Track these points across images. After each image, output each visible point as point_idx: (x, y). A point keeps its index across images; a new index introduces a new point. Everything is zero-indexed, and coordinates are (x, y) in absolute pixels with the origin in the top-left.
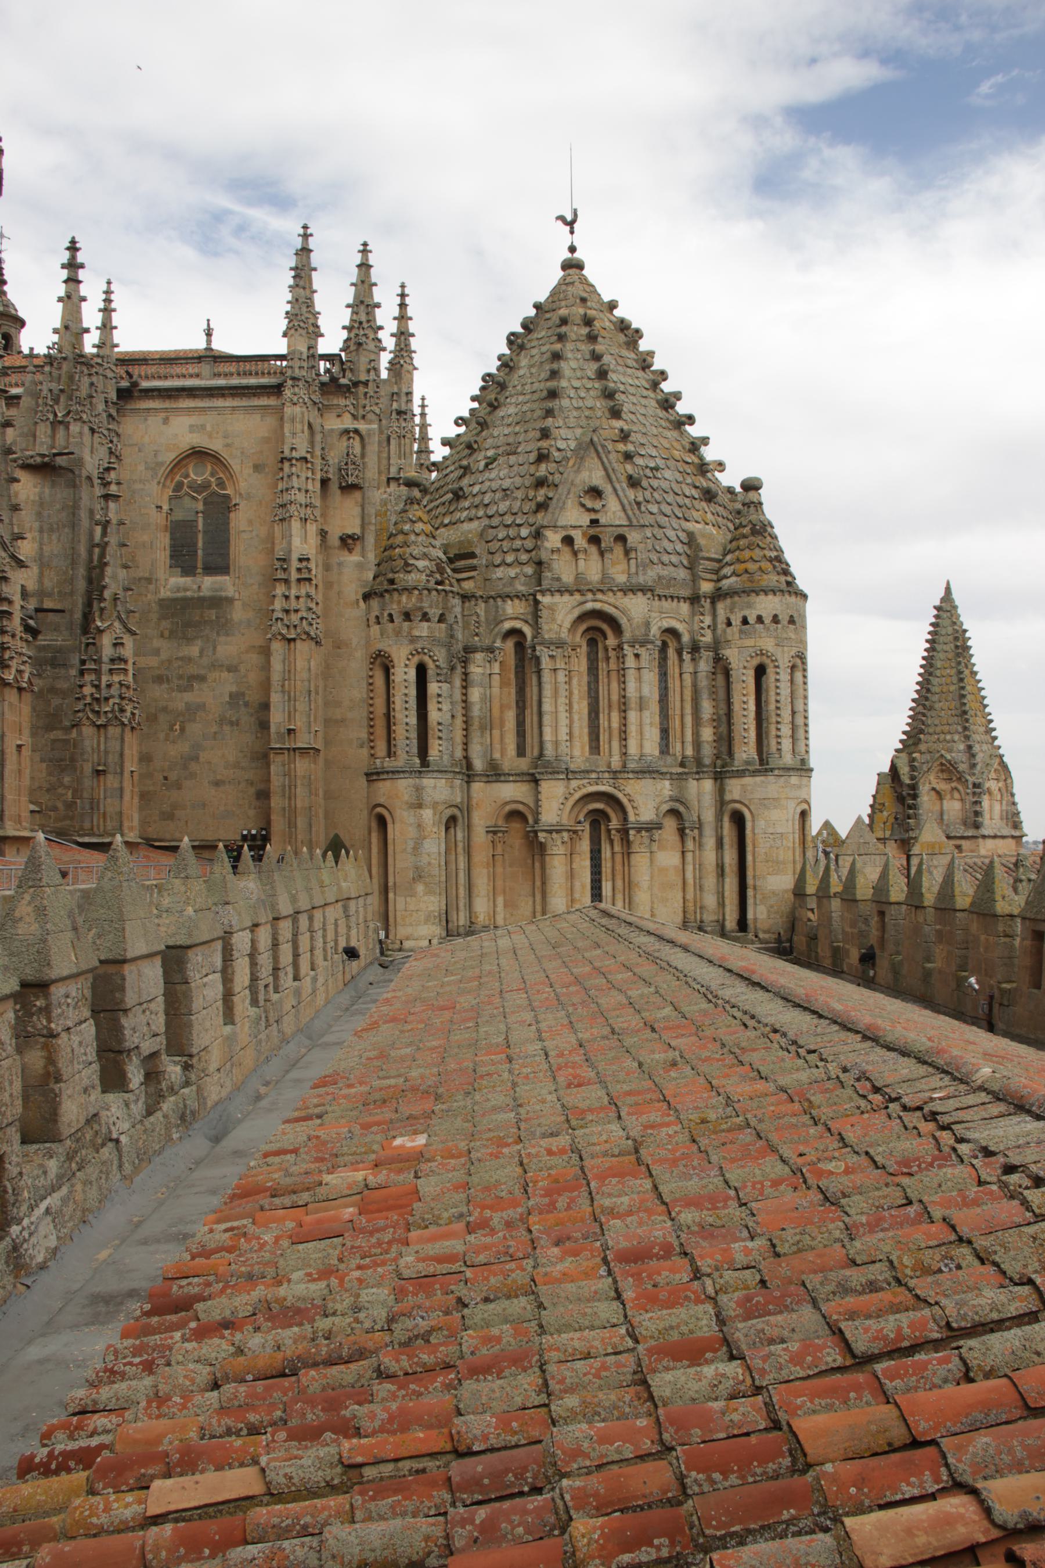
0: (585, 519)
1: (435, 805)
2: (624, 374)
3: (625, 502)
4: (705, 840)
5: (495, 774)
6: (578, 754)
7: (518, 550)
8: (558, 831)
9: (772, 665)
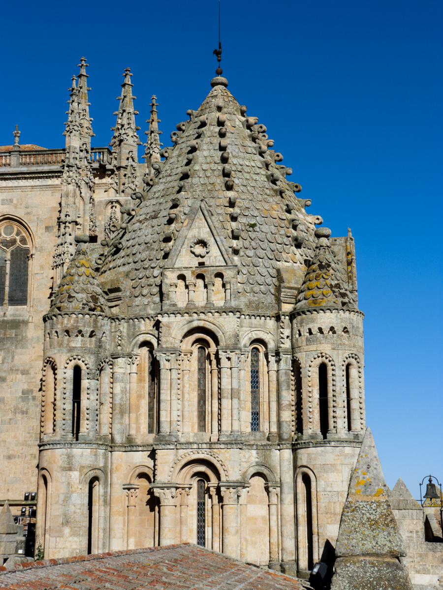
0: (195, 262)
1: (82, 467)
2: (244, 158)
3: (223, 249)
4: (284, 496)
5: (130, 445)
6: (188, 429)
7: (151, 285)
8: (168, 488)
9: (330, 364)
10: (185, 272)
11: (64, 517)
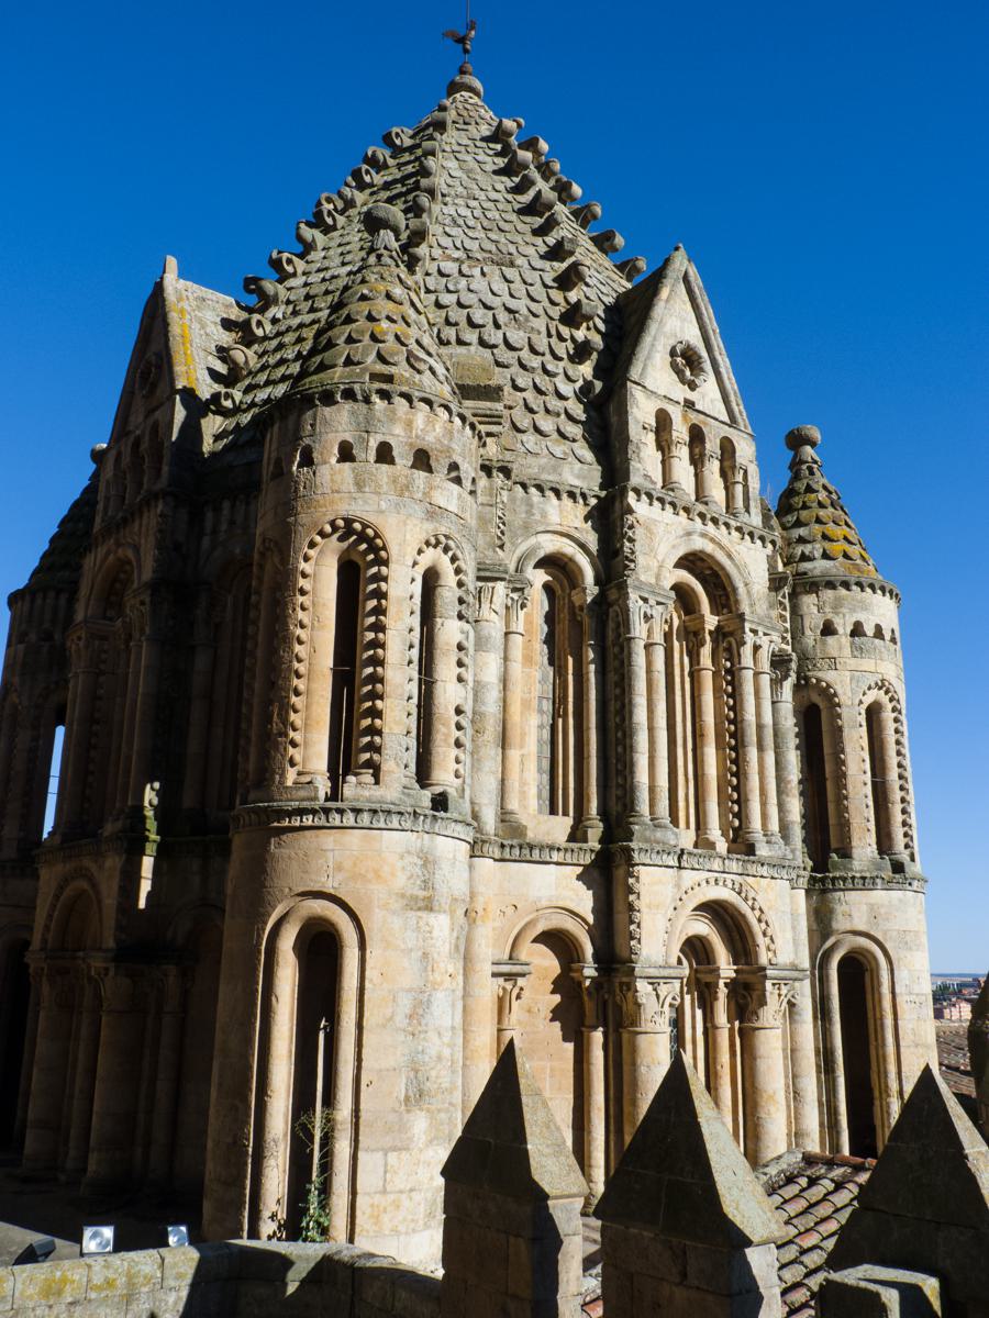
5: (515, 845)
10: (670, 409)
11: (412, 1074)
